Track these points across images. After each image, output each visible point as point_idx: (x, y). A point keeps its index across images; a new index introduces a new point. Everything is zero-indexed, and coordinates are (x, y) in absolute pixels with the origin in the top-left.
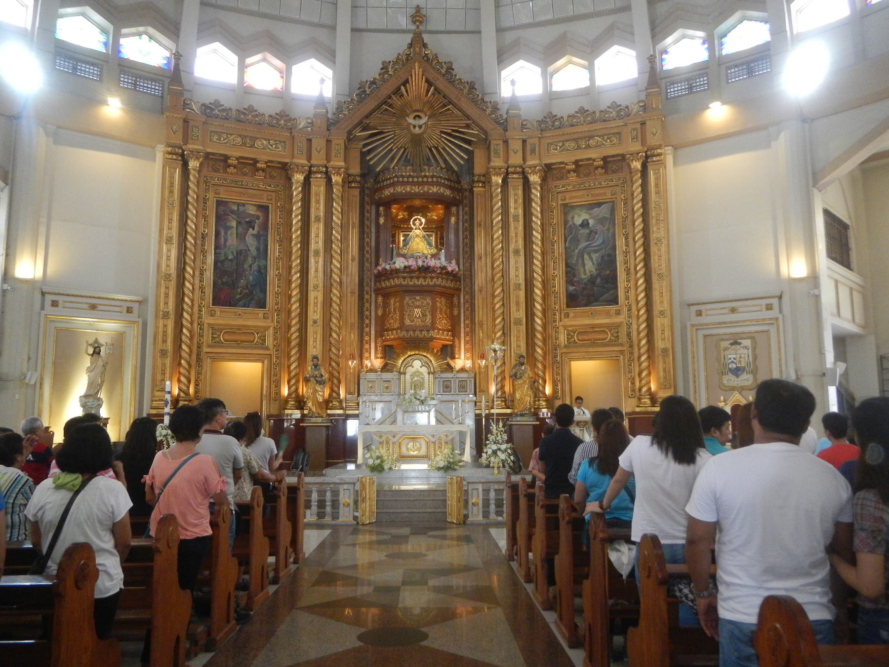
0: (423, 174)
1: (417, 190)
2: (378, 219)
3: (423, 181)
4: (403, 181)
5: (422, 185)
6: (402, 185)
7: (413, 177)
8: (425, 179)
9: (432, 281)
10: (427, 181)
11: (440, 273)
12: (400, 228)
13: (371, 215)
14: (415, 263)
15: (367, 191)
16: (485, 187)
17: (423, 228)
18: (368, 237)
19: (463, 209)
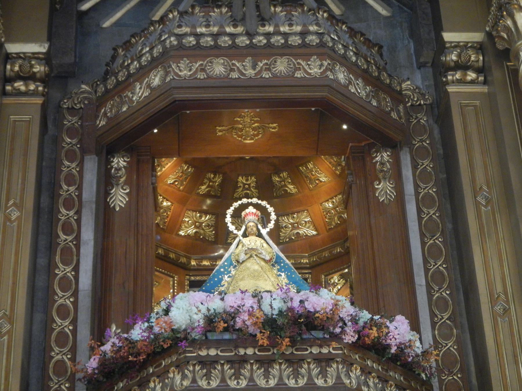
0: (270, 29)
1: (250, 72)
2: (107, 194)
3: (269, 45)
4: (198, 46)
5: (268, 56)
6: (193, 58)
7: (233, 36)
8: (278, 40)
9: (323, 374)
10: (286, 45)
11: (356, 346)
12: (185, 268)
13: (80, 188)
14: (250, 302)
15: (71, 121)
16: (485, 83)
17: (270, 234)
18: (66, 263)
19: (415, 167)
